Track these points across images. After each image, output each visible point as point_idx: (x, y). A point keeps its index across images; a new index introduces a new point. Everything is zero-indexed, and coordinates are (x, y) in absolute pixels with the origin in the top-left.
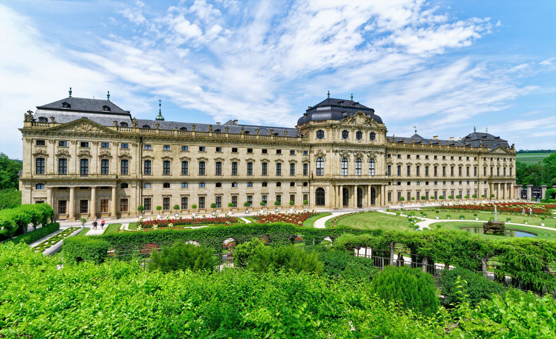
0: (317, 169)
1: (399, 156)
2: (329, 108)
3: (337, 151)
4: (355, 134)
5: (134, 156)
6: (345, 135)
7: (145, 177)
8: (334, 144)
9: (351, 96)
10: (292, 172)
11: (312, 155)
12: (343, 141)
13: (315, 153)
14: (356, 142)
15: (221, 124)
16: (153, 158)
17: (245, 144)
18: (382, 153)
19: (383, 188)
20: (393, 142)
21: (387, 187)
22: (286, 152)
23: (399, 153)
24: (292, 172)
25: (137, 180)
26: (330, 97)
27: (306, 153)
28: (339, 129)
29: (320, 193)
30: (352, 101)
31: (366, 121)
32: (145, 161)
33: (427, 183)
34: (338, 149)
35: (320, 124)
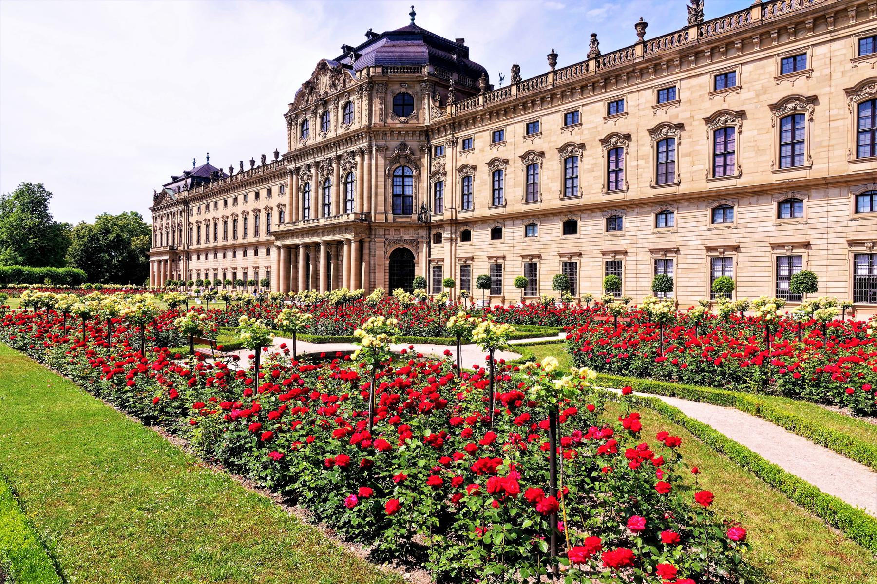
9: (410, 10)
21: (353, 245)
25: (184, 251)
30: (413, 25)
33: (570, 228)
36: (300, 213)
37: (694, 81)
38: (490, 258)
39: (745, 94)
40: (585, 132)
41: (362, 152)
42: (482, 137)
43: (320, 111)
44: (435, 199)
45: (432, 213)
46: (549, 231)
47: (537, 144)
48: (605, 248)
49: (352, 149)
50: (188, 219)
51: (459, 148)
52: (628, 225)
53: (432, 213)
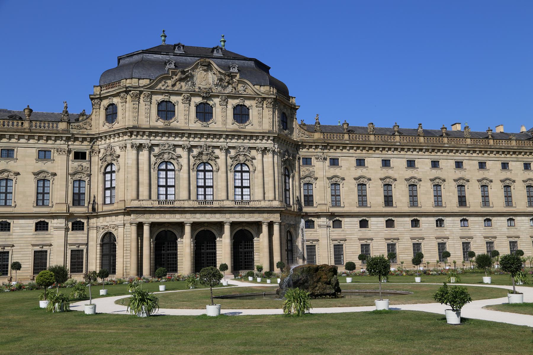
0: (106, 189)
1: (334, 162)
3: (140, 148)
4: (193, 109)
6: (166, 111)
8: (132, 131)
10: (42, 197)
11: (95, 159)
12: (160, 124)
13: (101, 155)
14: (196, 125)
18: (265, 151)
19: (265, 229)
20: (316, 131)
21: (276, 228)
23: (332, 153)
26: (167, 43)
27: (80, 156)
28: (150, 96)
29: (109, 243)
31: (221, 80)
34: (144, 140)
35: (111, 90)
37: (471, 162)
38: (360, 239)
39: (491, 174)
40: (421, 173)
41: (265, 151)
42: (348, 160)
43: (198, 100)
44: (305, 196)
45: (303, 205)
46: (403, 225)
47: (389, 172)
48: (436, 235)
49: (251, 145)
51: (328, 162)
52: (447, 224)
53: (303, 205)
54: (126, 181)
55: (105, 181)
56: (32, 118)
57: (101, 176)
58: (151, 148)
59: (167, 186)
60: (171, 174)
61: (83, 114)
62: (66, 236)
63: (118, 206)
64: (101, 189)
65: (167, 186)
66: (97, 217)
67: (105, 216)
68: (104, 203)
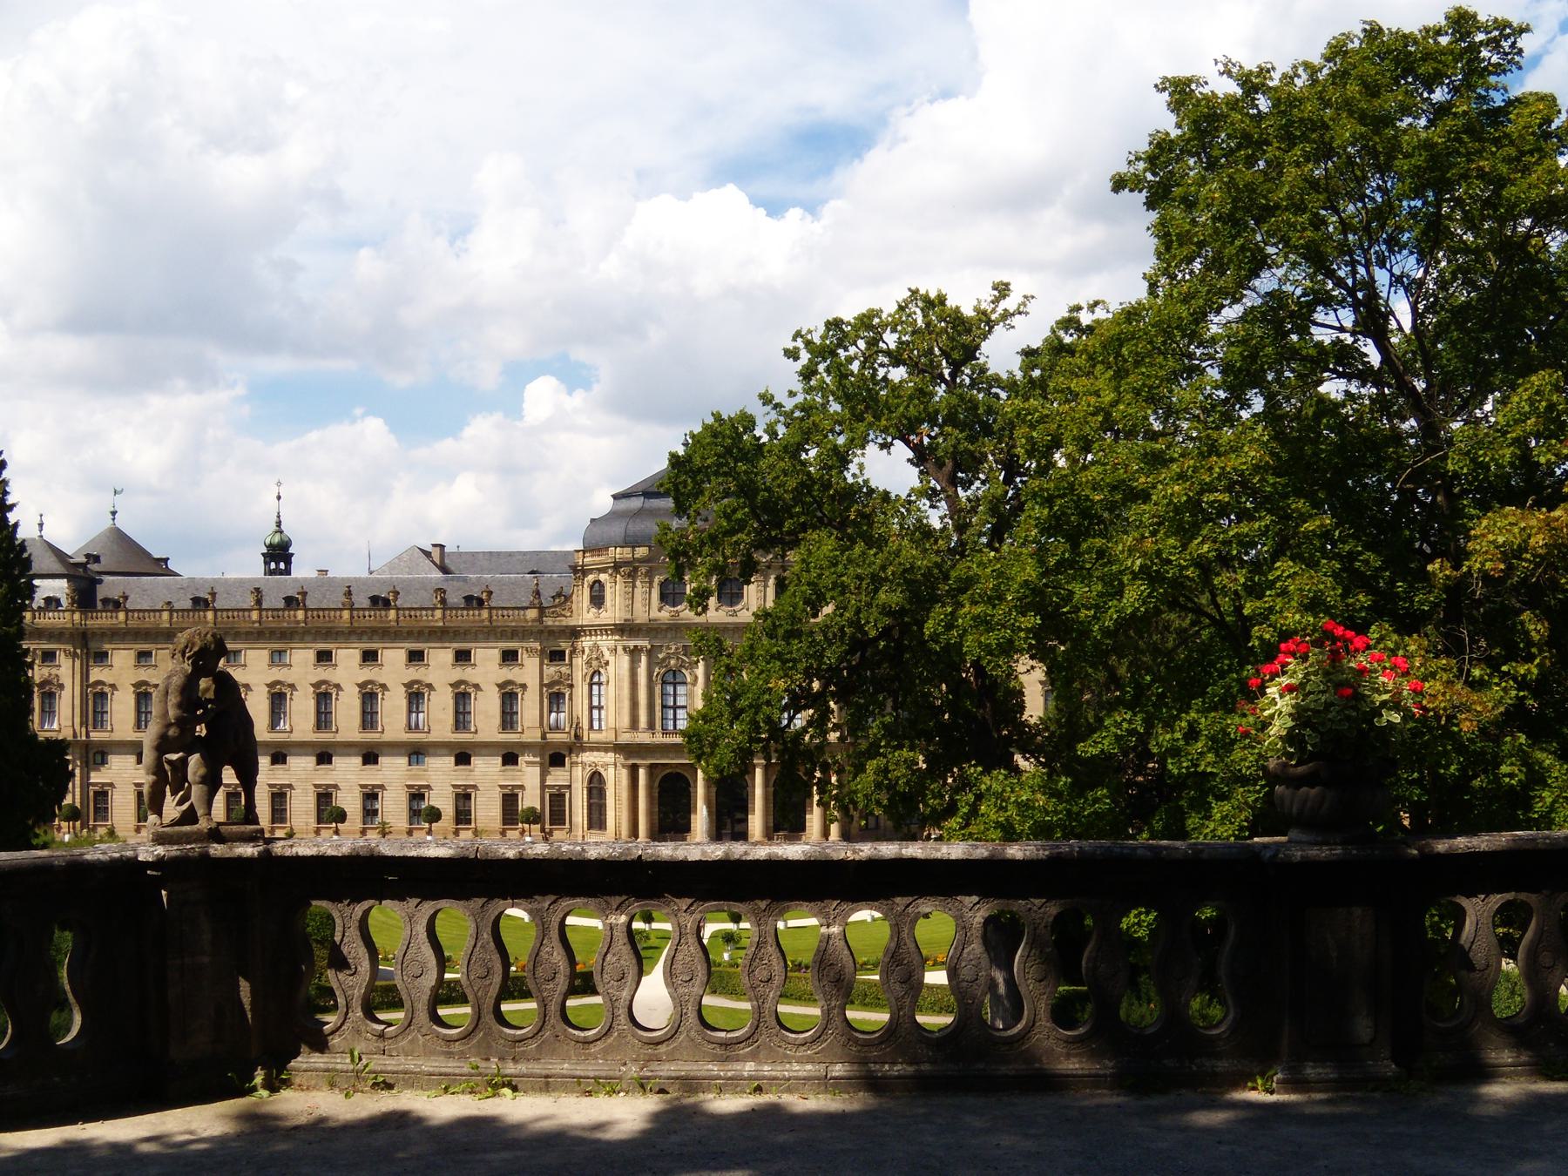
0: (591, 708)
2: (637, 503)
5: (67, 682)
7: (96, 736)
8: (626, 629)
10: (508, 718)
11: (579, 661)
12: (665, 615)
15: (330, 575)
16: (113, 686)
17: (353, 637)
22: (486, 657)
24: (508, 718)
27: (557, 656)
28: (650, 575)
32: (95, 694)
34: (644, 643)
35: (597, 559)
36: (658, 714)
50: (85, 675)
54: (617, 699)
55: (591, 696)
56: (493, 604)
57: (586, 688)
58: (650, 653)
59: (675, 707)
60: (681, 690)
61: (559, 595)
62: (544, 775)
63: (606, 736)
64: (586, 707)
65: (675, 707)
66: (583, 749)
67: (592, 749)
68: (591, 727)
